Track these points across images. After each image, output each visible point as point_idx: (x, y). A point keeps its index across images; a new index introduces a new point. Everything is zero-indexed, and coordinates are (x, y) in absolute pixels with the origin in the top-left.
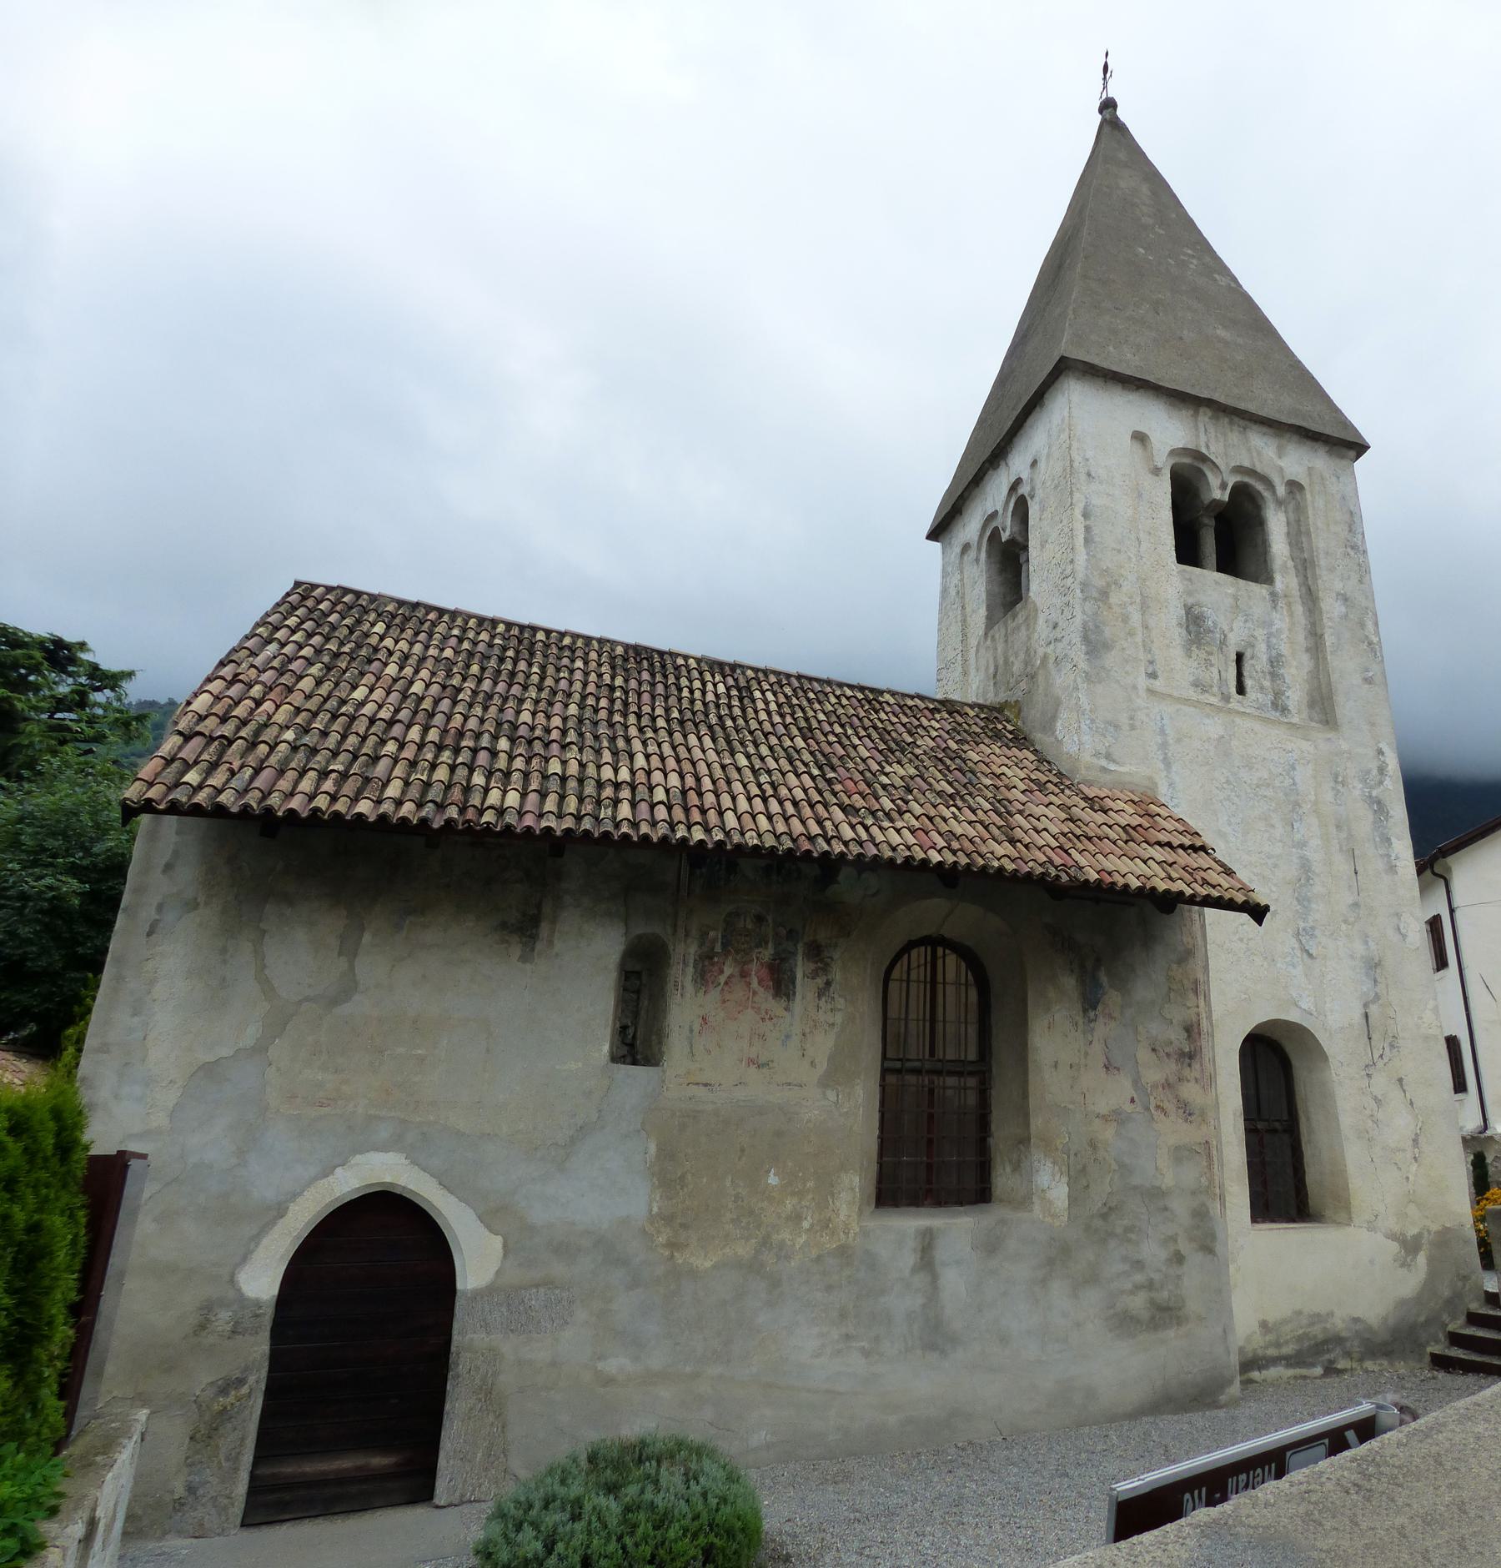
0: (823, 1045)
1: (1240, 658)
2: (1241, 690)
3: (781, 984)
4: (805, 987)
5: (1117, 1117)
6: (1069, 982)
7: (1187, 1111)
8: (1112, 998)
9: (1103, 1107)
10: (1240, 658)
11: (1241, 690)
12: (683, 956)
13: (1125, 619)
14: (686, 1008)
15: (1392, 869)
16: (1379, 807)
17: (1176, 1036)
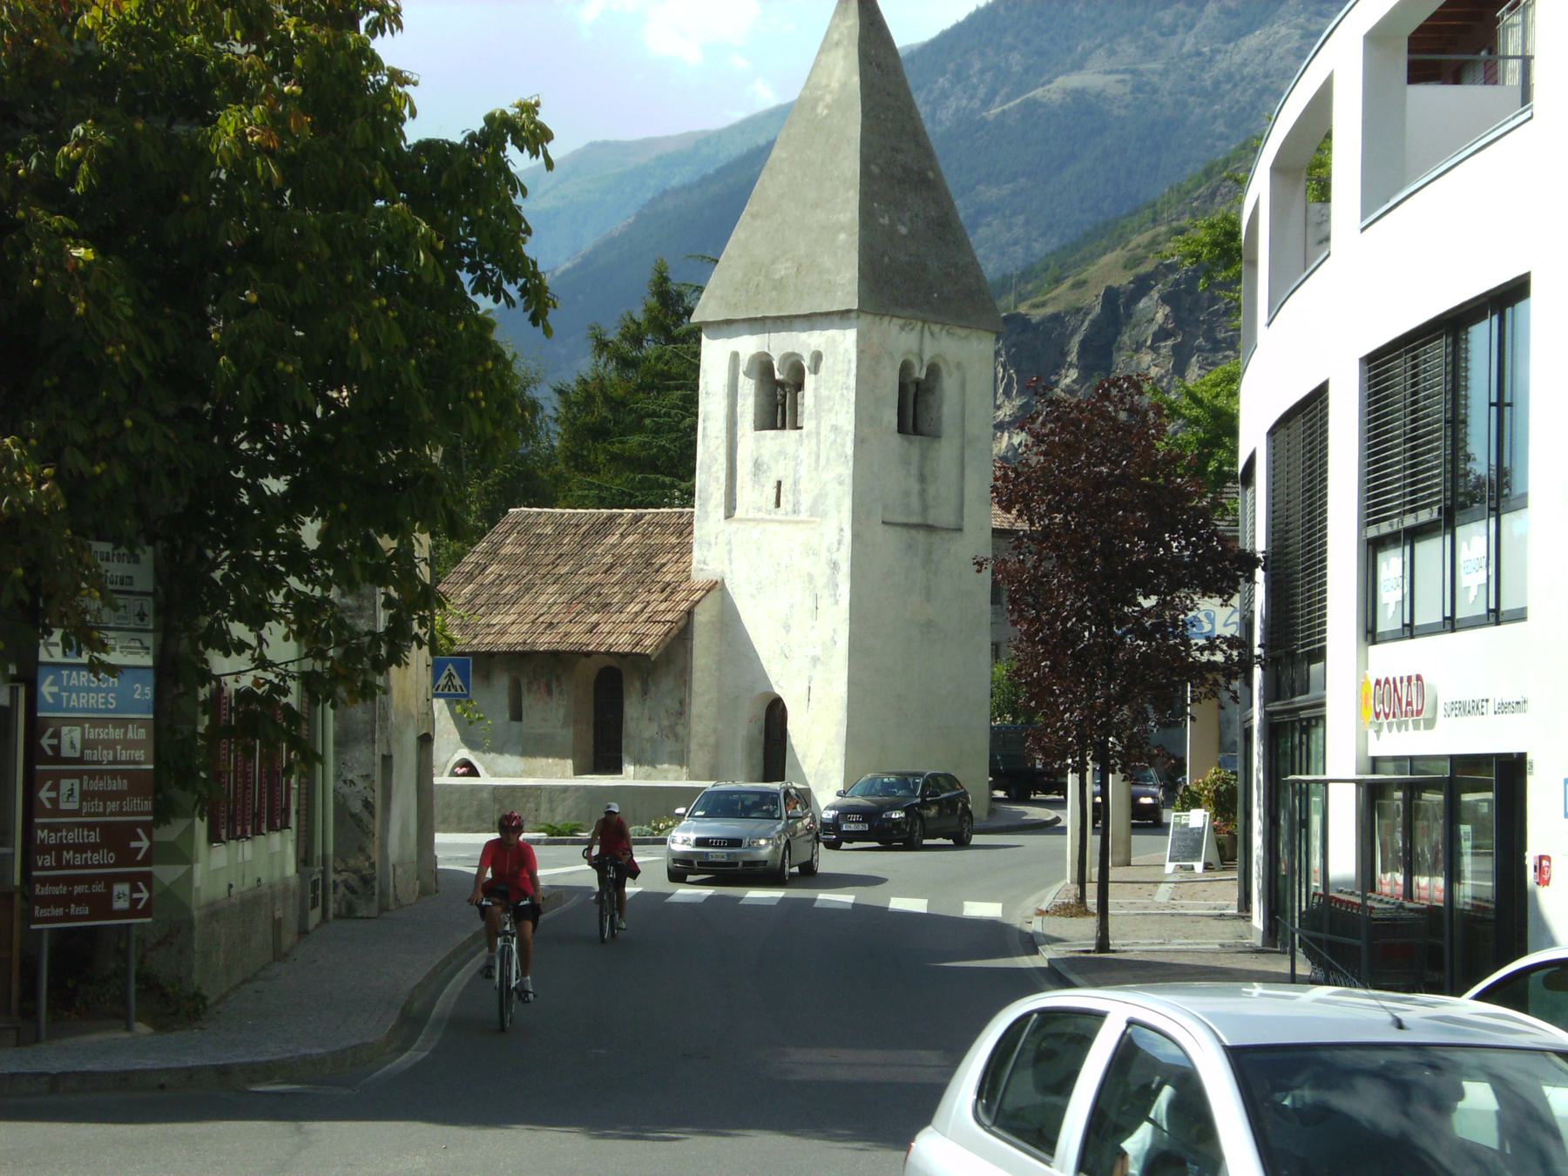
0: (561, 713)
1: (779, 483)
2: (778, 504)
3: (550, 692)
4: (555, 691)
5: (652, 740)
6: (638, 684)
7: (676, 737)
8: (653, 689)
9: (647, 735)
10: (779, 483)
11: (778, 504)
12: (524, 681)
13: (717, 479)
14: (527, 701)
15: (837, 602)
16: (835, 566)
17: (677, 705)
